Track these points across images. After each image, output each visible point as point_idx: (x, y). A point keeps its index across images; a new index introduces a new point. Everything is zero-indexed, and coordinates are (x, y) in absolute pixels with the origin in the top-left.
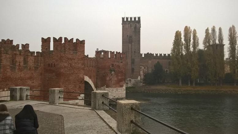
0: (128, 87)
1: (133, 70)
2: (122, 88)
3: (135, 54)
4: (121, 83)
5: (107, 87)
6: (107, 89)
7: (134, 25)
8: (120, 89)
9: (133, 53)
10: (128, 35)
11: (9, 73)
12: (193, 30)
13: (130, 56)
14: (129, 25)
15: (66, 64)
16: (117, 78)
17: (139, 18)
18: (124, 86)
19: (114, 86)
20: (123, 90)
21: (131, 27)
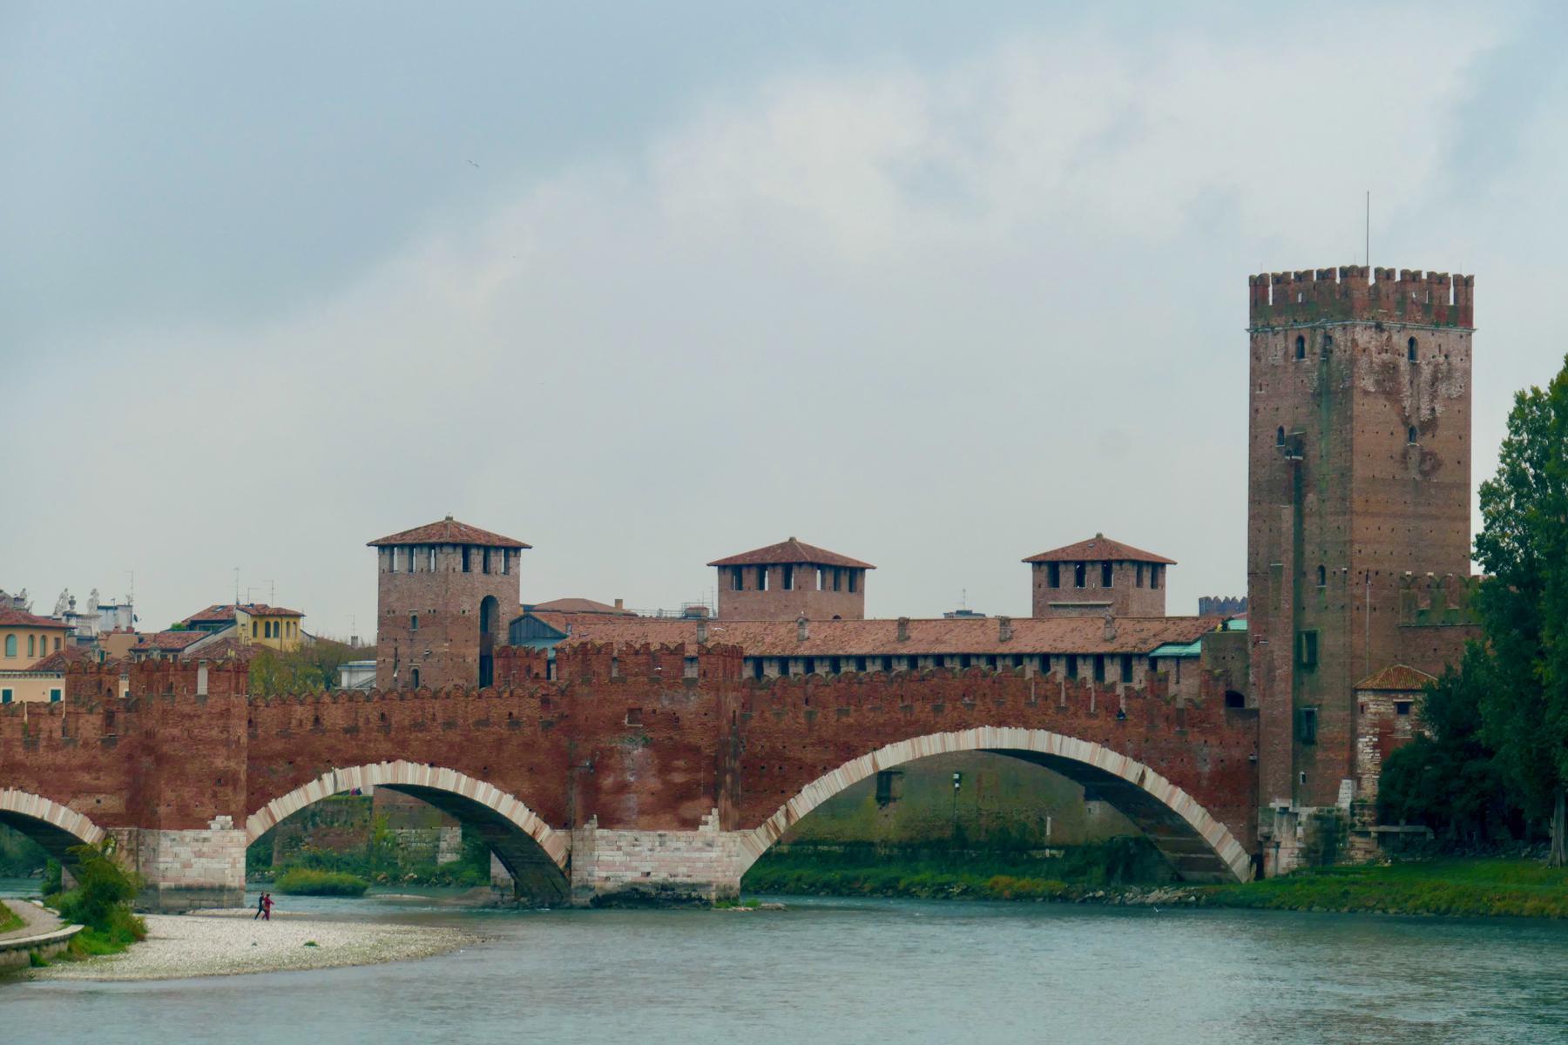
0: (1280, 871)
1: (1305, 724)
2: (690, 833)
3: (1321, 590)
4: (688, 809)
5: (601, 826)
6: (605, 832)
7: (1319, 339)
8: (678, 839)
9: (1313, 577)
11: (20, 754)
13: (1287, 606)
14: (1292, 348)
15: (176, 732)
16: (665, 782)
18: (706, 823)
19: (644, 820)
20: (700, 845)
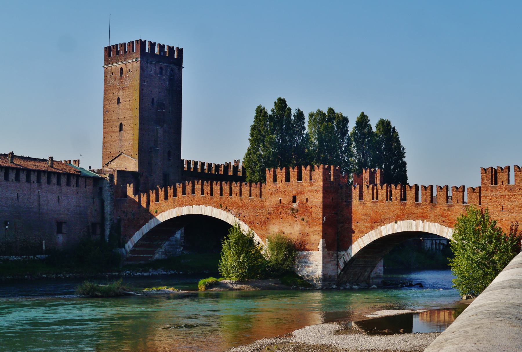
7: (169, 70)
9: (166, 155)
10: (153, 99)
12: (294, 112)
14: (158, 70)
17: (180, 51)
21: (161, 74)
